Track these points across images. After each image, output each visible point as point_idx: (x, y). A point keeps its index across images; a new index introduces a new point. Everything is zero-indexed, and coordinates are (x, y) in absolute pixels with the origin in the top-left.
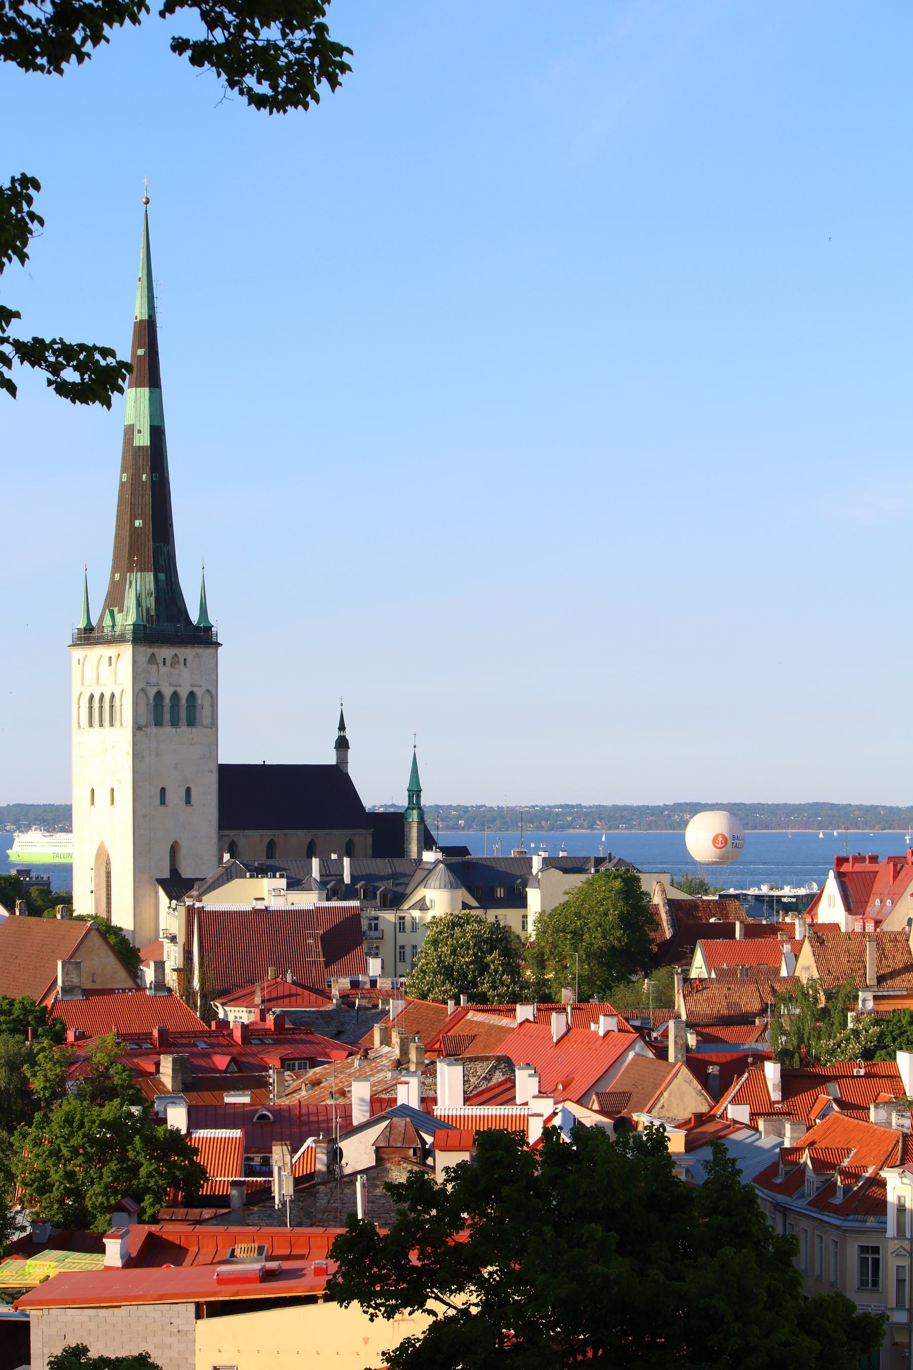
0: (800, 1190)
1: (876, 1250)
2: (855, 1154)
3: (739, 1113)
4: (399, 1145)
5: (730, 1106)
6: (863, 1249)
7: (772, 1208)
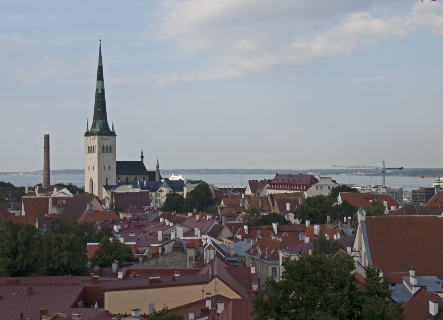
0: (257, 255)
1: (276, 268)
2: (269, 247)
3: (239, 237)
4: (178, 247)
5: (237, 235)
6: (273, 268)
7: (251, 259)
